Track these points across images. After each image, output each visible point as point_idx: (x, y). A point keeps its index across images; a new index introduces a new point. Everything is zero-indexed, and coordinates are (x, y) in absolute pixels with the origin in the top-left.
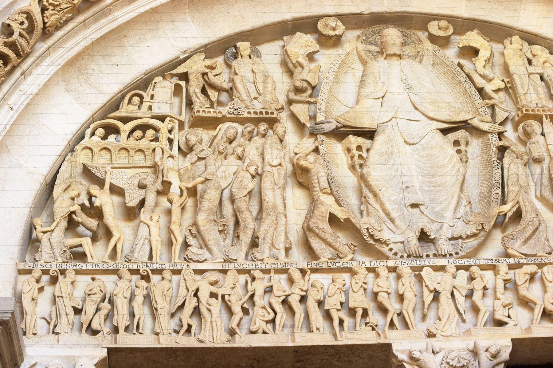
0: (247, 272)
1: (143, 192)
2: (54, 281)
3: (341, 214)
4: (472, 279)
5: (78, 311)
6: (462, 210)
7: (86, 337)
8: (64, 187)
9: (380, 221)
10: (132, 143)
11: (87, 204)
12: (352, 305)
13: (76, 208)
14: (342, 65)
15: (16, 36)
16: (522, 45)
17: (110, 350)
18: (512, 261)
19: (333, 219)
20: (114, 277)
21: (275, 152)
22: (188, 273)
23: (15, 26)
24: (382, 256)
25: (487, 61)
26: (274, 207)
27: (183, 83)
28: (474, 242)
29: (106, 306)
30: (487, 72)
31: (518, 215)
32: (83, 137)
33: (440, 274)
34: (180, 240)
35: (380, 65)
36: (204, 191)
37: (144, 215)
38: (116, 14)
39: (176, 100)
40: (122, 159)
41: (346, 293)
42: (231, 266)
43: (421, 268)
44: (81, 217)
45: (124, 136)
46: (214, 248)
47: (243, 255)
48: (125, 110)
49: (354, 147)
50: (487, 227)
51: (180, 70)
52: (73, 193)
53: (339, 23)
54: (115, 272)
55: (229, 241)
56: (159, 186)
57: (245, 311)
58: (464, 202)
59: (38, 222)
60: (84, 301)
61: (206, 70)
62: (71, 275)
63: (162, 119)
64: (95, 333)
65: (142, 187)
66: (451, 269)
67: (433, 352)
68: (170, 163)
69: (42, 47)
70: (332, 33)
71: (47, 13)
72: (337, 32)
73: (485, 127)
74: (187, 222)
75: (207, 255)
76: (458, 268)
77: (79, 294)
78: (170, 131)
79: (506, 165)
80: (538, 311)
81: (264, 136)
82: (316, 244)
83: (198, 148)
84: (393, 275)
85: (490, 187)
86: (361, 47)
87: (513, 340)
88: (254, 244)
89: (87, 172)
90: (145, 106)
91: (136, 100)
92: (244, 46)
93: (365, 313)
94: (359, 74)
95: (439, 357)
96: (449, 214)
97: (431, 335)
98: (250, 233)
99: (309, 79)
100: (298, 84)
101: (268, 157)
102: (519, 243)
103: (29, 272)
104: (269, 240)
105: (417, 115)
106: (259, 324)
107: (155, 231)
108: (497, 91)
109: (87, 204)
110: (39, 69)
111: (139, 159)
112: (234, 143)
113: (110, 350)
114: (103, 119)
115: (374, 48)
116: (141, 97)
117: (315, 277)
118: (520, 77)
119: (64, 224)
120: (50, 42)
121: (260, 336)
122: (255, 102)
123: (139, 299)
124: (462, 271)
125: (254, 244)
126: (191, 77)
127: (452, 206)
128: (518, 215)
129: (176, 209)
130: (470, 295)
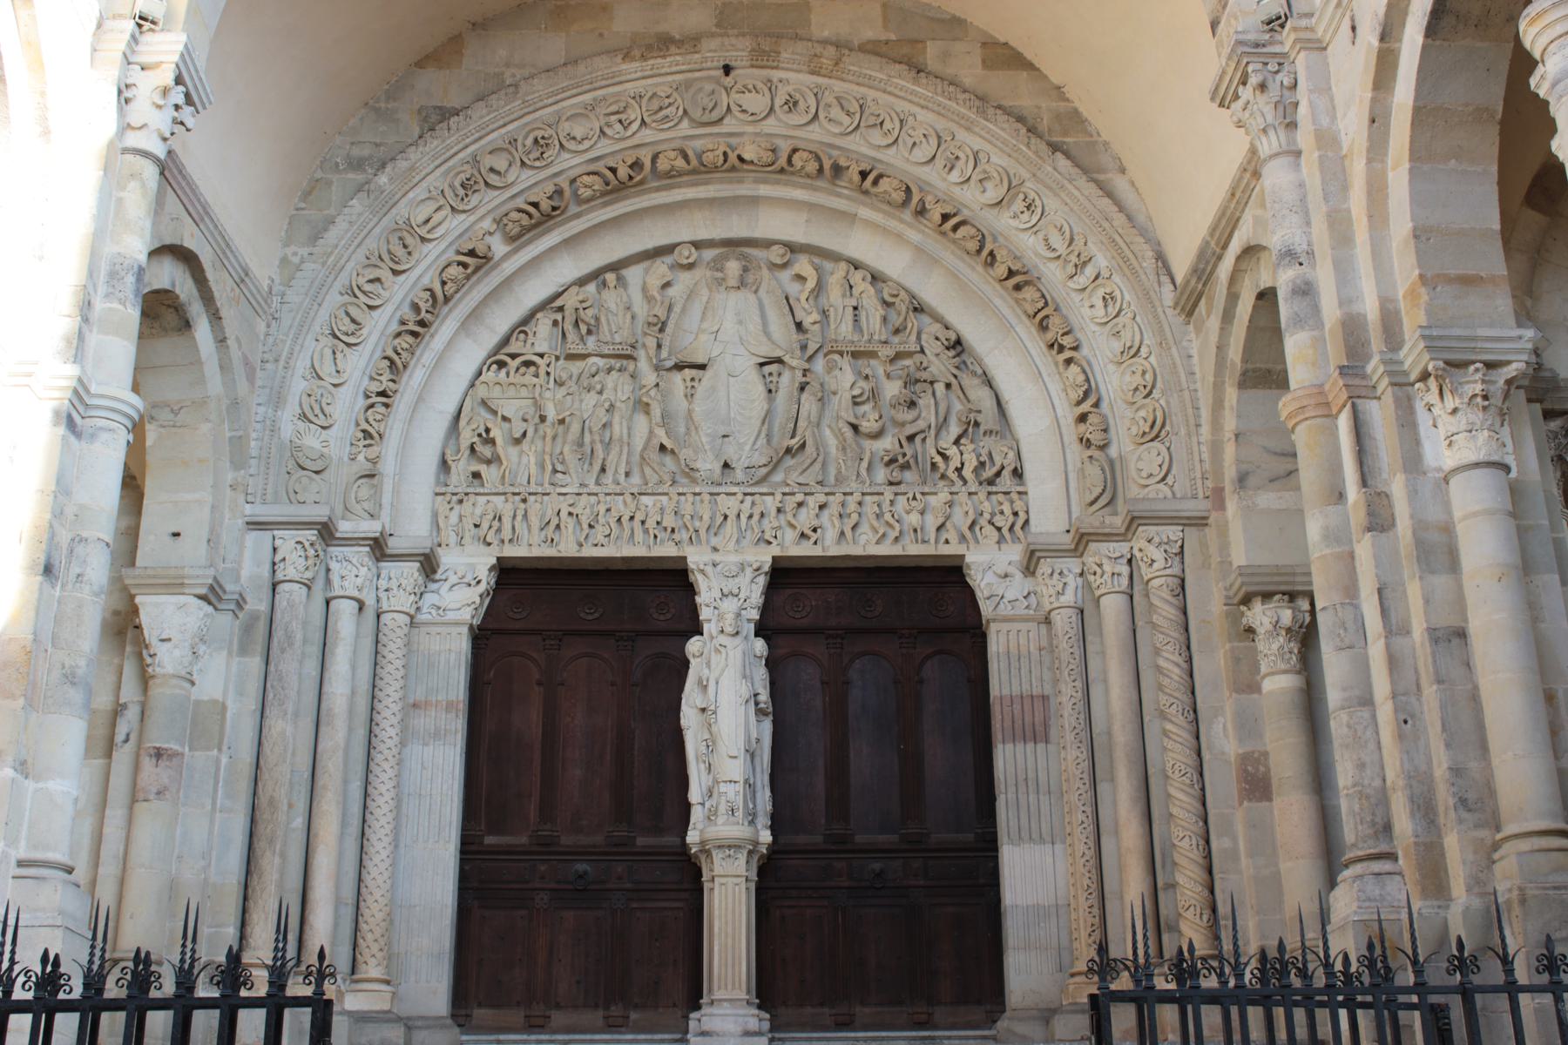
0: (596, 494)
1: (525, 424)
2: (461, 502)
3: (669, 445)
4: (753, 503)
5: (476, 526)
6: (759, 443)
7: (483, 547)
8: (467, 419)
9: (696, 452)
10: (517, 379)
11: (484, 435)
12: (664, 524)
13: (476, 439)
14: (691, 295)
15: (423, 314)
16: (848, 273)
17: (498, 559)
18: (787, 490)
19: (662, 448)
20: (503, 498)
21: (626, 387)
22: (554, 496)
23: (422, 304)
24: (694, 481)
25: (812, 291)
26: (621, 440)
27: (559, 317)
28: (764, 471)
29: (496, 523)
30: (807, 306)
31: (803, 446)
32: (480, 374)
33: (732, 498)
34: (550, 467)
35: (721, 296)
36: (570, 424)
37: (525, 444)
38: (505, 265)
39: (555, 329)
40: (512, 392)
41: (662, 514)
42: (585, 490)
43: (718, 494)
44: (479, 448)
45: (512, 373)
46: (574, 476)
47: (594, 480)
48: (514, 347)
49: (688, 379)
50: (775, 460)
51: (558, 303)
52: (474, 426)
53: (693, 249)
54: (505, 494)
55: (586, 466)
56: (537, 420)
57: (591, 526)
58: (763, 435)
59: (448, 452)
60: (481, 517)
61: (579, 306)
62: (472, 497)
63: (541, 356)
64: (489, 544)
65: (525, 420)
66: (740, 497)
67: (714, 565)
68: (548, 394)
69: (446, 309)
70: (685, 262)
71: (446, 288)
72: (691, 260)
73: (794, 363)
74: (558, 451)
75: (569, 480)
76: (745, 494)
77: (478, 511)
78: (548, 365)
79: (802, 401)
80: (797, 533)
81: (620, 370)
82: (648, 470)
83: (569, 383)
84: (698, 498)
85: (788, 420)
86: (709, 273)
87: (774, 558)
88: (603, 470)
89: (484, 403)
90: (529, 342)
91: (522, 336)
92: (610, 277)
93: (673, 531)
94: (705, 299)
95: (719, 567)
96: (747, 448)
97: (715, 549)
98: (600, 462)
99: (659, 314)
100: (651, 320)
101: (620, 393)
102: (797, 473)
103: (443, 494)
104: (613, 469)
105: (742, 351)
106: (600, 538)
107: (533, 460)
108: (815, 323)
109: (484, 435)
110: (444, 328)
111: (524, 392)
112: (596, 378)
113: (498, 559)
114: (495, 355)
115: (719, 275)
116: (525, 332)
117: (644, 499)
118: (836, 310)
119: (468, 452)
120: (451, 304)
121: (599, 548)
122: (616, 336)
123: (519, 518)
124: (748, 497)
125: (603, 470)
126: (567, 313)
127: (752, 439)
128: (803, 446)
129: (548, 439)
130: (751, 517)
